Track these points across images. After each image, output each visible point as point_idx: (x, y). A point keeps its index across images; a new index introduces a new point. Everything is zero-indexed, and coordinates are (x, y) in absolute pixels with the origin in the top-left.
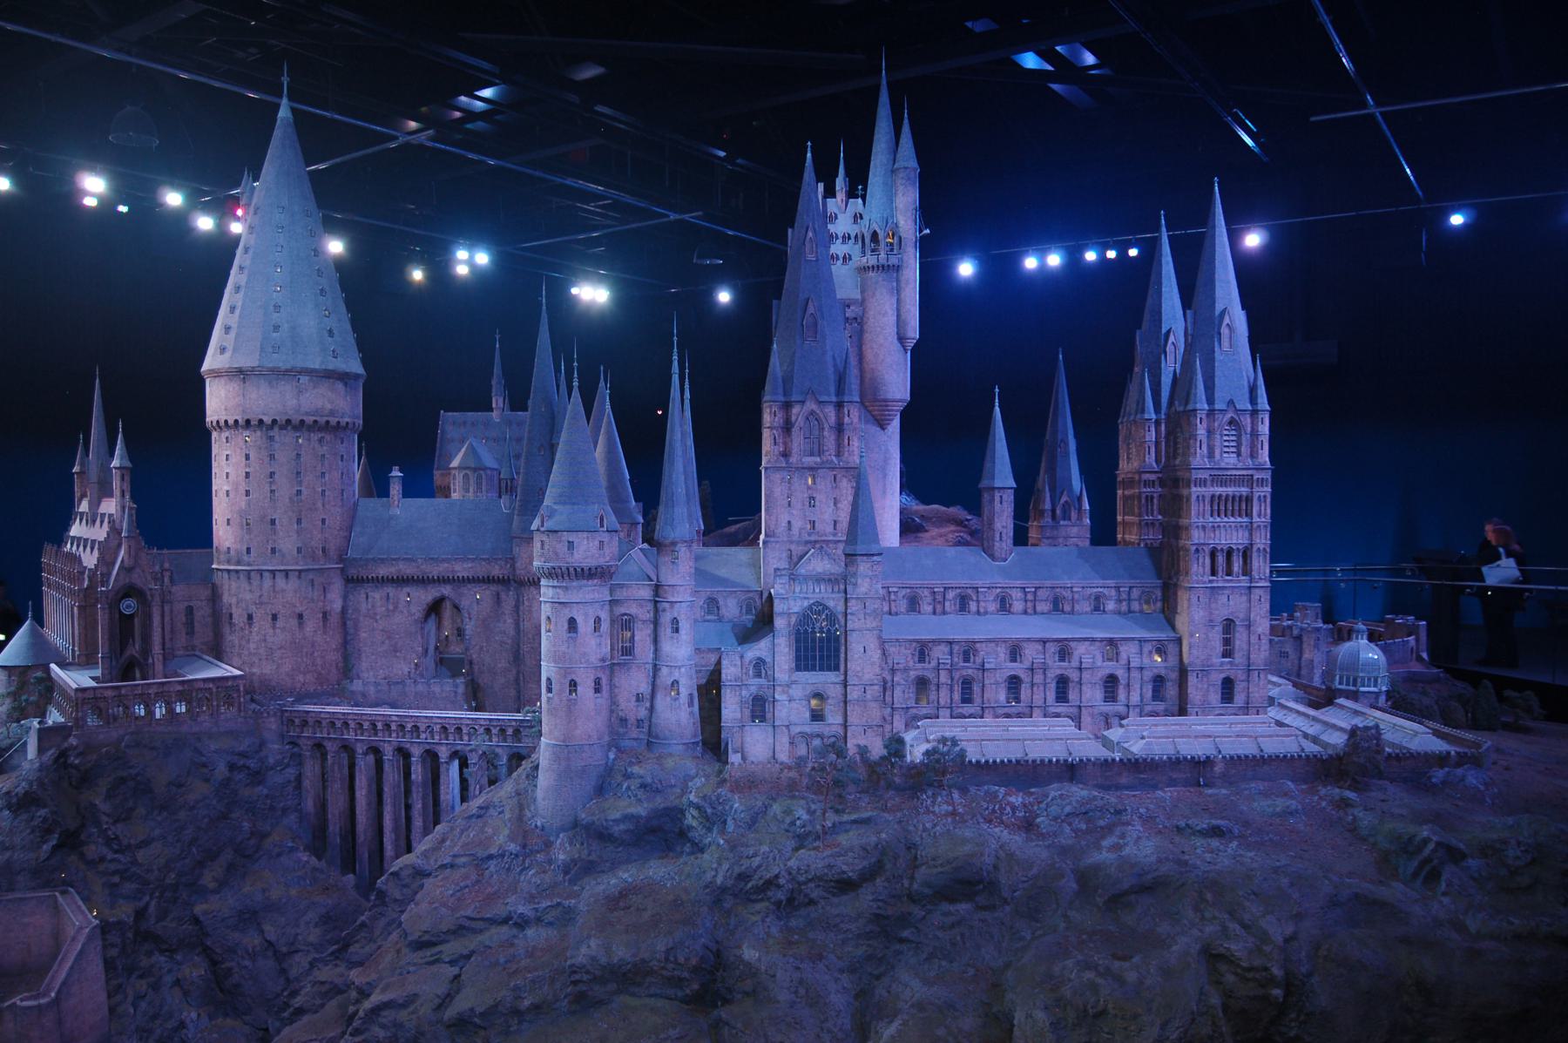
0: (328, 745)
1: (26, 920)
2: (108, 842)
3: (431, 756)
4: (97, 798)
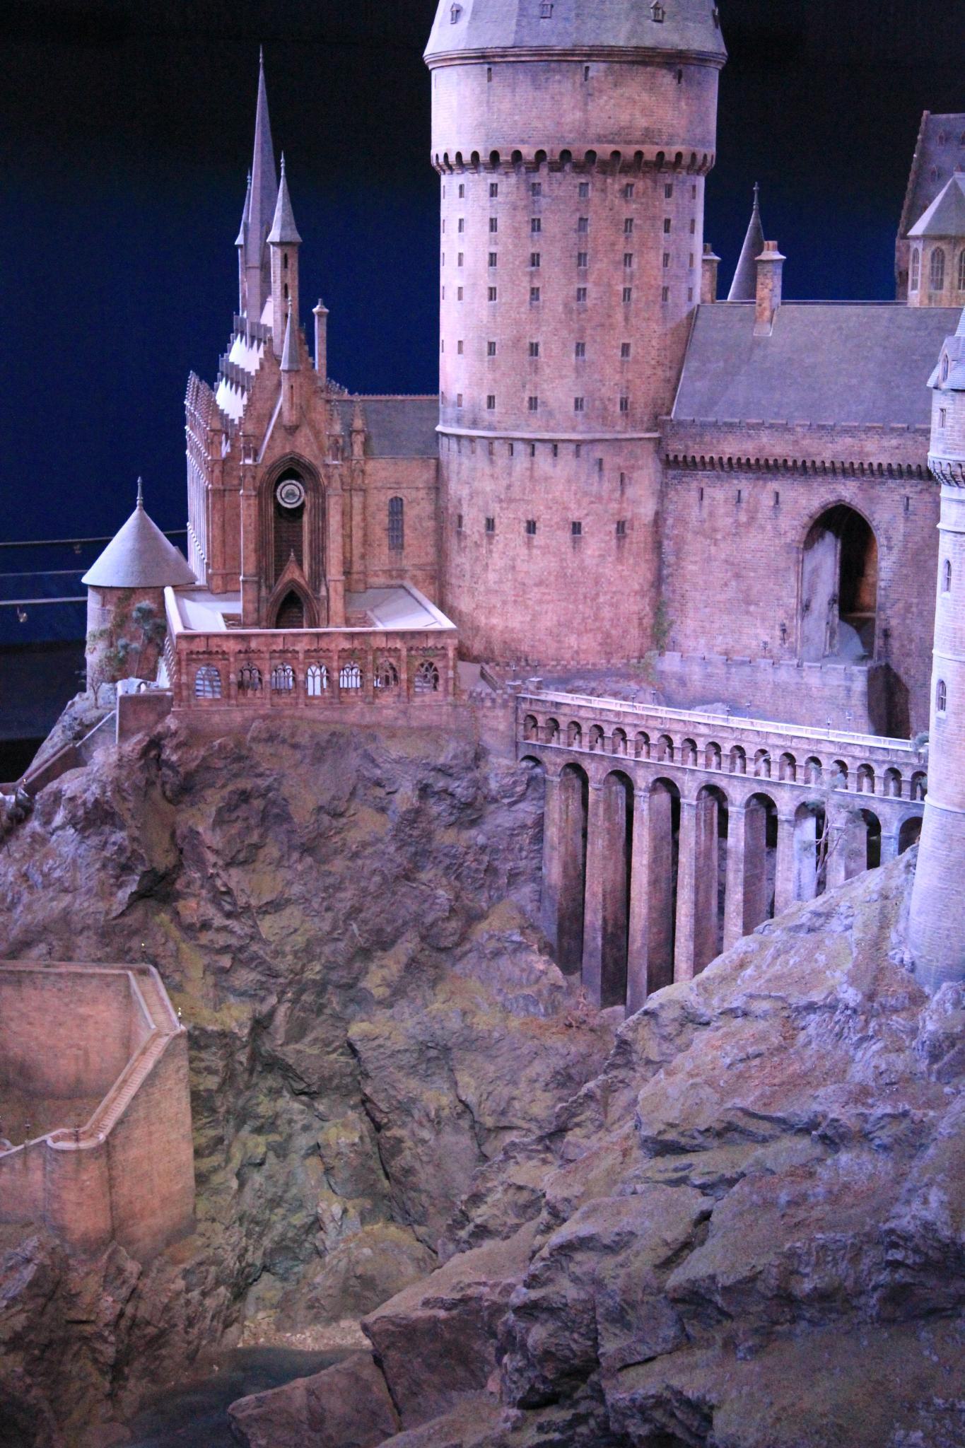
0: (590, 768)
1: (82, 1010)
2: (218, 897)
3: (763, 804)
4: (201, 820)
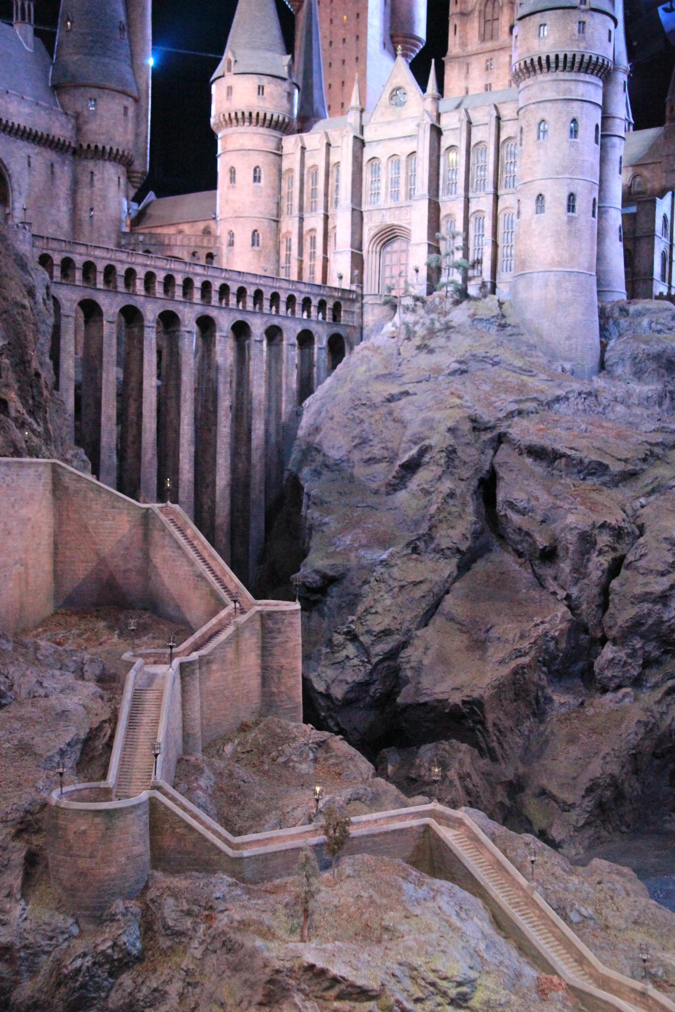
1: (24, 512)
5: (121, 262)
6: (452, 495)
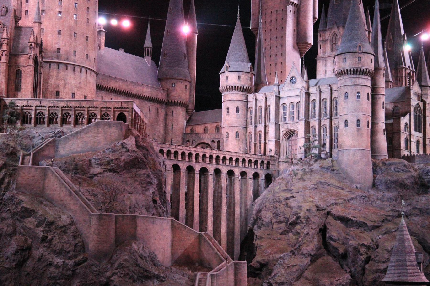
5: (187, 150)
6: (308, 234)
